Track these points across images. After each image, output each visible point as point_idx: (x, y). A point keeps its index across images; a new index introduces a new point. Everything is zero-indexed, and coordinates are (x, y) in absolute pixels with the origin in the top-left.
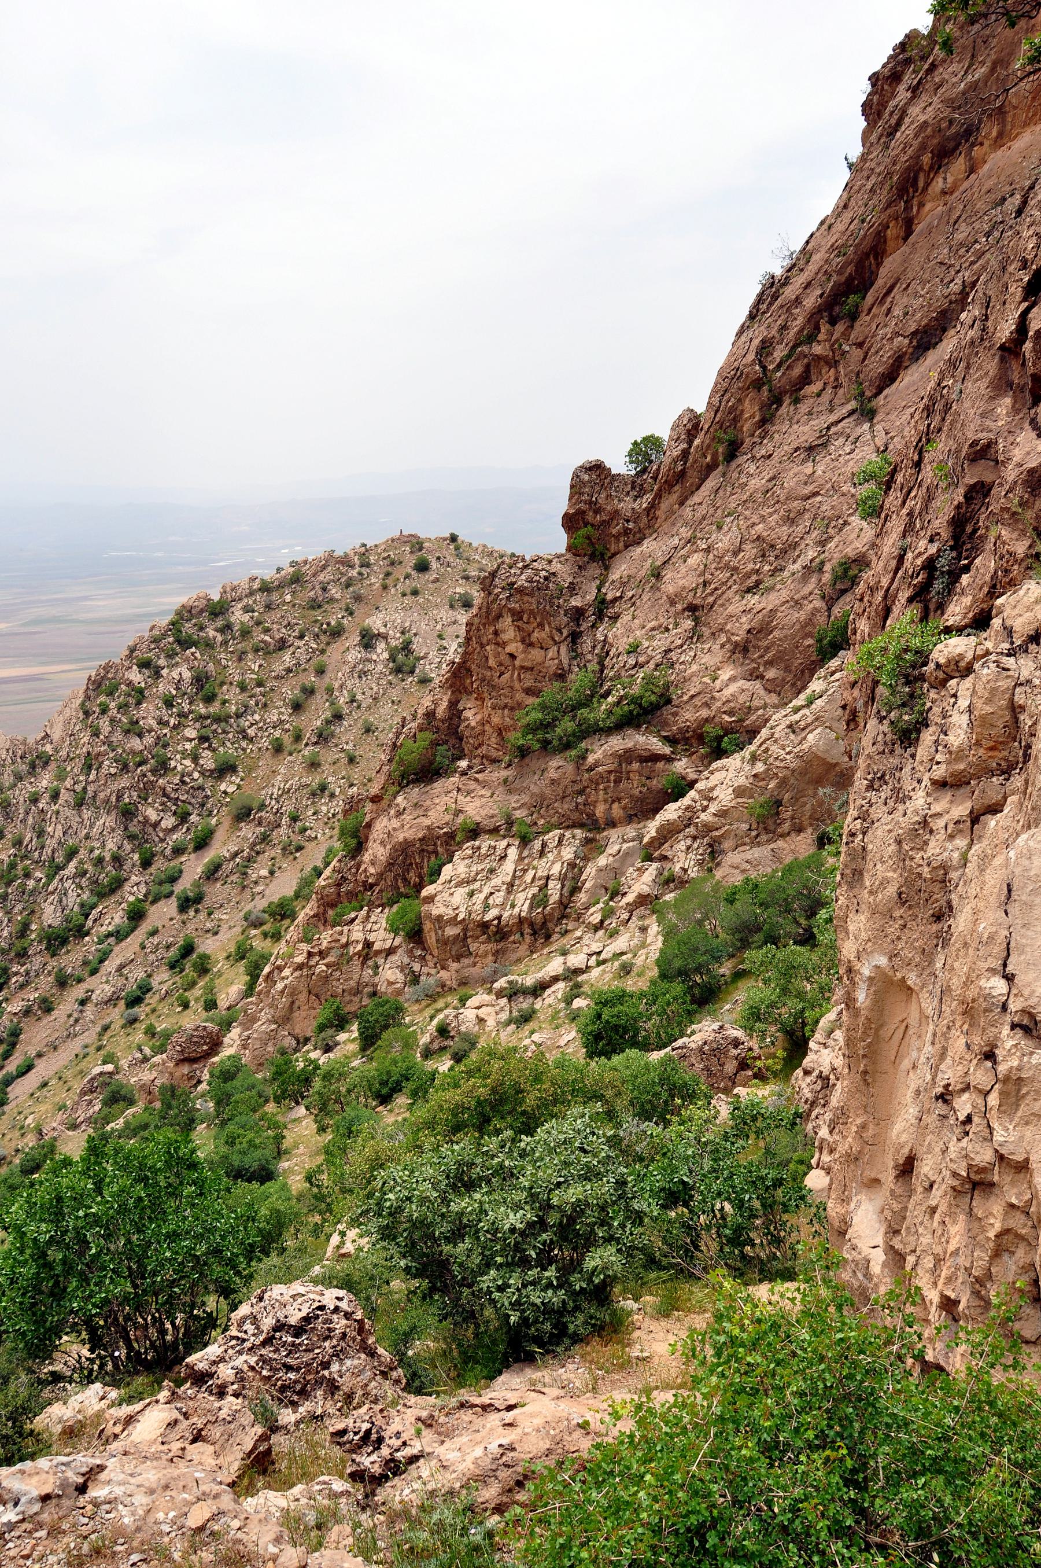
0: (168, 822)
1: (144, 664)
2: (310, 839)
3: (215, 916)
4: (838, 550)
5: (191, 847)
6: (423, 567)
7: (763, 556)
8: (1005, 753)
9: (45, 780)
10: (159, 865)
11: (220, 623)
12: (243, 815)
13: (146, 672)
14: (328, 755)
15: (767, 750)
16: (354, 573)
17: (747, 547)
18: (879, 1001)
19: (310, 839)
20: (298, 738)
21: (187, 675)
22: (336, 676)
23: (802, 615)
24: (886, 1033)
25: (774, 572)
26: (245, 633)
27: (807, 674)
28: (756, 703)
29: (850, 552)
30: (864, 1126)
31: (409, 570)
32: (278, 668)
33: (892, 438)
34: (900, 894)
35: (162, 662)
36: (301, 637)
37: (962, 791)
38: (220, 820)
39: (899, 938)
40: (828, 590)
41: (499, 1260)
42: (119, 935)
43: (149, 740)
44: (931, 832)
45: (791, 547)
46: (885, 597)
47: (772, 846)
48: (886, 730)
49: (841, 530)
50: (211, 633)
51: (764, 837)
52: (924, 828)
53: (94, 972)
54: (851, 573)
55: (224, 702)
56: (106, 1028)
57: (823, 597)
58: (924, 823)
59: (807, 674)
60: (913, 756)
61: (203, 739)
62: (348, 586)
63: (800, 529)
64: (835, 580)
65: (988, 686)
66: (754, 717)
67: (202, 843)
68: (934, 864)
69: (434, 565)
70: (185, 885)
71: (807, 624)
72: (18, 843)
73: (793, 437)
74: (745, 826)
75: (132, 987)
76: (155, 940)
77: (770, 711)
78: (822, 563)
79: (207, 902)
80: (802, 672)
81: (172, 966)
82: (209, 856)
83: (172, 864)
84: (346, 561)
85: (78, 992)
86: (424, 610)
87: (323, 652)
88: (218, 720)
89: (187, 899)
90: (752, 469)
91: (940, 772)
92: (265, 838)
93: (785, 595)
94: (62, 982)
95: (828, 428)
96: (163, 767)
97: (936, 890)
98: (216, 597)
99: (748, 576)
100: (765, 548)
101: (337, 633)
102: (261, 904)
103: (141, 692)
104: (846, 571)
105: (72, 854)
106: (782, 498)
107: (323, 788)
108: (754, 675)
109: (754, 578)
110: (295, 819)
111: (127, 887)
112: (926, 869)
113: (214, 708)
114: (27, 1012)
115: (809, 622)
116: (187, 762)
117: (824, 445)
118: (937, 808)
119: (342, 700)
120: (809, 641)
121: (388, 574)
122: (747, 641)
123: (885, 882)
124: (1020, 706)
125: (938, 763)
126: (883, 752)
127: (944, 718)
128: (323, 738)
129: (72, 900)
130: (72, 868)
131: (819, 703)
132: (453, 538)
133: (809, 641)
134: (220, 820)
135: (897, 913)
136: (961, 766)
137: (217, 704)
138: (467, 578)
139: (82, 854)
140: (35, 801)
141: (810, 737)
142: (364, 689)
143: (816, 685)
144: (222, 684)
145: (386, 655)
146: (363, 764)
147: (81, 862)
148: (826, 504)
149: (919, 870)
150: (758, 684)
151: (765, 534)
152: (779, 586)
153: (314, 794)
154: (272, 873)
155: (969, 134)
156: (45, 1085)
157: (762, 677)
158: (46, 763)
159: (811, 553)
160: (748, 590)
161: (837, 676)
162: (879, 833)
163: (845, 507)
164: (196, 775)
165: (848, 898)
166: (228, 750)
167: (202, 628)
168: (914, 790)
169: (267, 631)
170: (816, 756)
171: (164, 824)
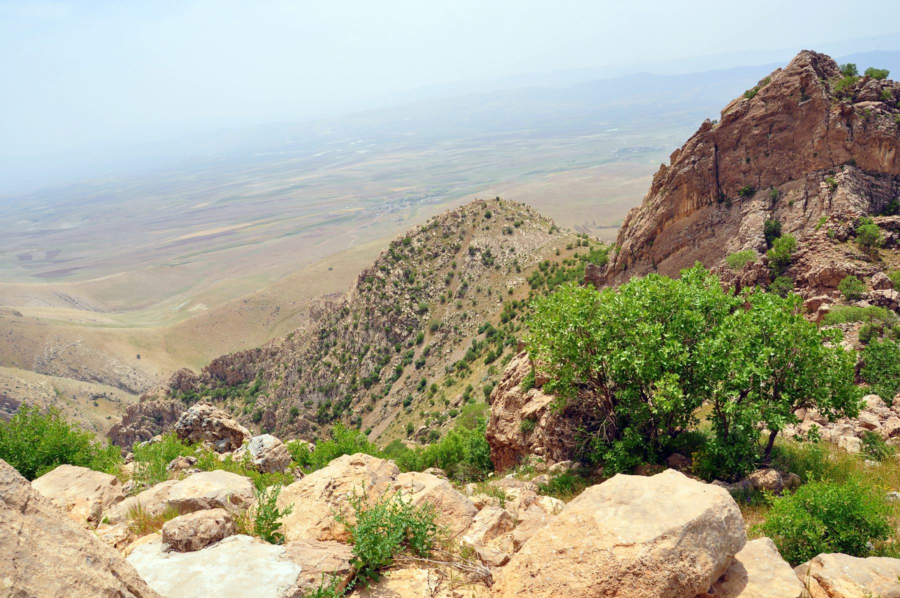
0: (405, 333)
1: (383, 269)
2: (464, 336)
3: (432, 368)
6: (488, 216)
9: (349, 320)
10: (403, 351)
11: (409, 248)
12: (434, 329)
14: (465, 302)
16: (460, 220)
19: (464, 336)
20: (450, 296)
21: (401, 272)
22: (461, 268)
26: (420, 252)
32: (437, 266)
35: (390, 267)
36: (443, 251)
38: (425, 331)
42: (394, 380)
43: (391, 301)
53: (386, 394)
56: (398, 415)
61: (413, 299)
67: (420, 341)
69: (493, 214)
70: (417, 358)
72: (343, 346)
75: (404, 399)
81: (419, 390)
82: (424, 347)
84: (455, 215)
85: (383, 402)
88: (417, 290)
92: (445, 338)
96: (399, 312)
98: (405, 237)
101: (457, 249)
102: (452, 363)
103: (384, 281)
105: (367, 350)
107: (465, 316)
110: (456, 329)
111: (392, 360)
113: (414, 286)
114: (362, 412)
119: (466, 278)
121: (474, 220)
128: (461, 295)
129: (372, 367)
130: (369, 353)
132: (498, 199)
134: (425, 331)
138: (507, 219)
139: (372, 349)
140: (347, 329)
146: (479, 305)
153: (462, 319)
155: (672, 217)
156: (379, 437)
158: (348, 314)
166: (423, 302)
167: (402, 251)
169: (429, 250)
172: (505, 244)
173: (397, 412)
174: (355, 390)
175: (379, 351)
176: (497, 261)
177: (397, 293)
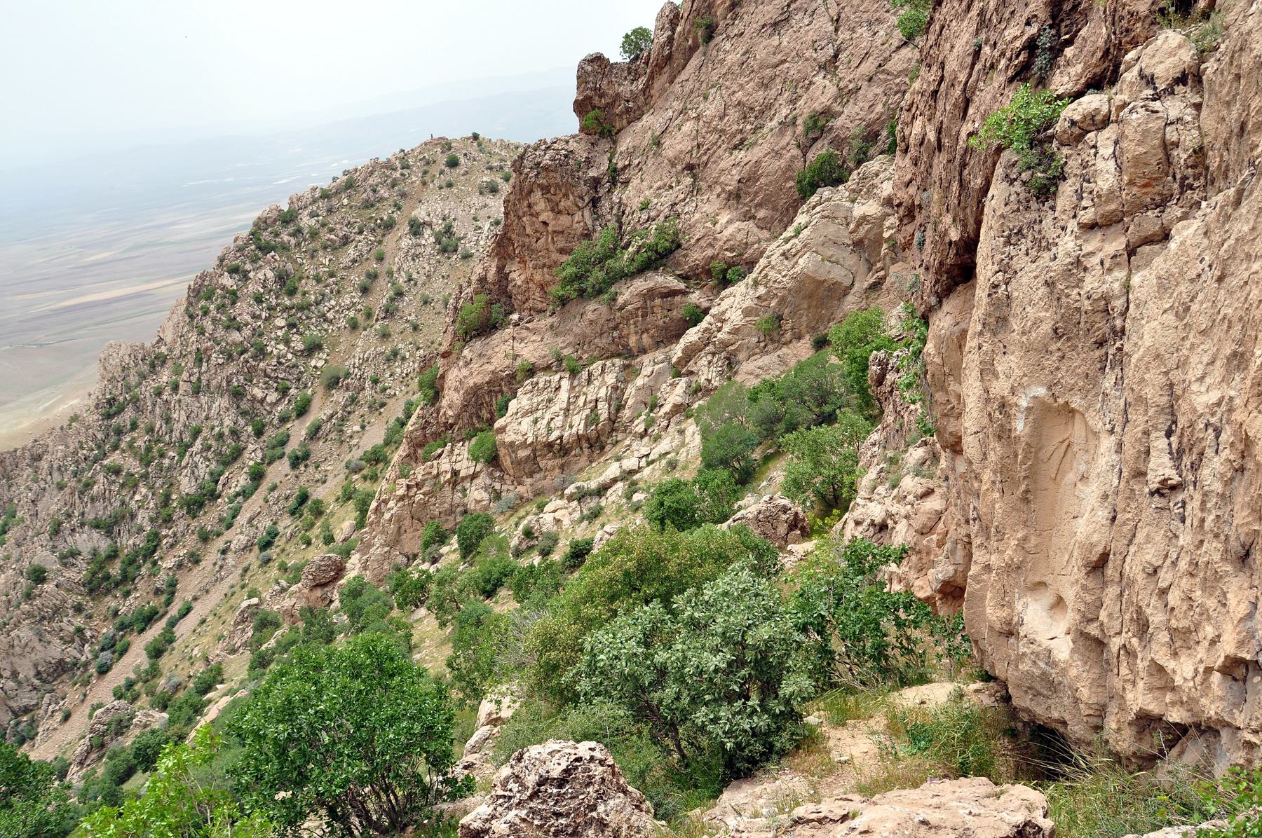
1: (234, 270)
2: (390, 397)
4: (806, 107)
5: (294, 415)
6: (453, 163)
7: (745, 118)
8: (1158, 189)
9: (165, 376)
10: (270, 433)
11: (291, 228)
12: (333, 383)
13: (237, 277)
14: (395, 327)
15: (766, 275)
16: (397, 175)
17: (731, 111)
18: (1037, 429)
19: (390, 397)
20: (369, 315)
21: (270, 275)
22: (394, 261)
23: (782, 163)
24: (1044, 455)
25: (755, 131)
26: (314, 235)
27: (791, 211)
28: (751, 239)
29: (818, 106)
30: (1025, 539)
31: (443, 167)
32: (345, 260)
33: (843, 8)
34: (1055, 331)
35: (248, 267)
36: (361, 232)
37: (1112, 229)
38: (315, 390)
39: (1058, 369)
40: (802, 140)
41: (707, 697)
42: (245, 494)
43: (247, 332)
44: (1086, 269)
45: (766, 109)
46: (964, 90)
47: (779, 353)
48: (1019, 190)
49: (808, 89)
50: (286, 238)
51: (771, 347)
52: (1077, 267)
53: (229, 526)
54: (820, 124)
55: (304, 293)
56: (246, 570)
57: (799, 146)
58: (1078, 262)
59: (791, 211)
60: (1053, 208)
61: (291, 326)
62: (393, 186)
63: (773, 92)
64: (808, 130)
65: (1139, 129)
66: (751, 251)
67: (302, 411)
68: (1095, 296)
69: (462, 160)
70: (293, 446)
71: (787, 170)
72: (150, 430)
73: (760, 16)
74: (754, 340)
76: (276, 494)
77: (764, 244)
78: (795, 118)
79: (313, 458)
80: (787, 209)
81: (293, 513)
82: (309, 420)
83: (281, 431)
84: (389, 166)
85: (219, 544)
86: (459, 199)
87: (380, 242)
88: (301, 308)
89: (297, 458)
90: (728, 46)
91: (1087, 216)
92: (353, 400)
93: (766, 147)
94: (205, 538)
95: (789, 5)
96: (261, 353)
97: (1098, 320)
99: (734, 135)
100: (746, 111)
101: (389, 226)
102: (360, 453)
103: (234, 293)
104: (815, 122)
105: (196, 433)
106: (756, 67)
107: (395, 353)
108: (748, 217)
109: (739, 137)
110: (375, 382)
111: (246, 455)
112: (1087, 302)
113: (297, 299)
114: (180, 566)
115: (789, 167)
116: (281, 346)
117: (787, 20)
118: (1088, 248)
120: (791, 184)
121: (425, 173)
122: (739, 189)
123: (1037, 322)
124: (1173, 143)
125: (1085, 208)
126: (1018, 210)
127: (1085, 168)
128: (389, 313)
129: (203, 471)
130: (198, 445)
131: (806, 232)
132: (476, 137)
133: (791, 184)
134: (315, 390)
135: (1053, 347)
136: (1113, 207)
137: (299, 296)
138: (490, 168)
139: (205, 432)
140: (159, 393)
141: (801, 261)
142: (418, 269)
143: (801, 219)
144: (301, 279)
145: (432, 239)
146: (425, 331)
147: (205, 439)
148: (793, 70)
149: (1077, 305)
150: (751, 223)
151: (744, 99)
152: (760, 141)
154: (363, 427)
156: (203, 621)
157: (754, 217)
158: (164, 362)
159: (785, 111)
160: (735, 148)
161: (818, 209)
162: (1024, 280)
163: (810, 69)
164: (290, 356)
165: (993, 343)
166: (314, 332)
167: (277, 235)
168: (1059, 237)
169: (331, 230)
170: (807, 276)
171: (269, 399)
172: (483, 213)
173: (246, 564)
174: (168, 520)
175: (221, 436)
176: (466, 245)
177: (259, 317)
